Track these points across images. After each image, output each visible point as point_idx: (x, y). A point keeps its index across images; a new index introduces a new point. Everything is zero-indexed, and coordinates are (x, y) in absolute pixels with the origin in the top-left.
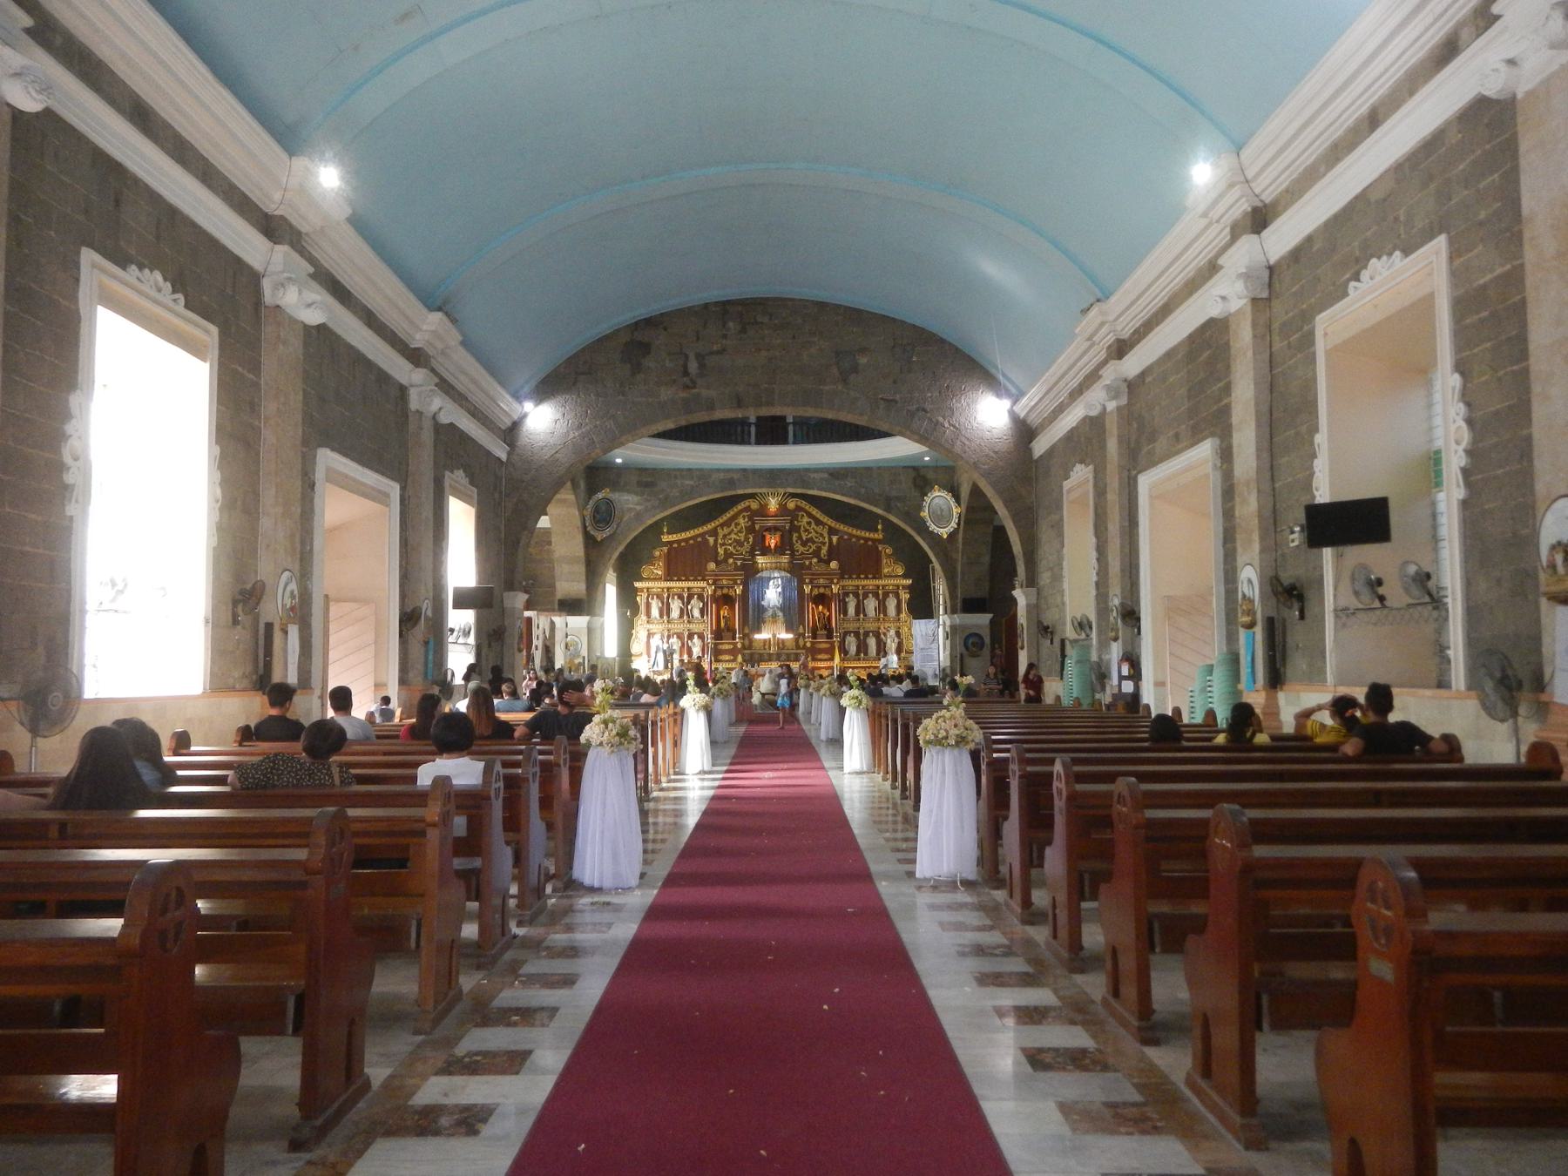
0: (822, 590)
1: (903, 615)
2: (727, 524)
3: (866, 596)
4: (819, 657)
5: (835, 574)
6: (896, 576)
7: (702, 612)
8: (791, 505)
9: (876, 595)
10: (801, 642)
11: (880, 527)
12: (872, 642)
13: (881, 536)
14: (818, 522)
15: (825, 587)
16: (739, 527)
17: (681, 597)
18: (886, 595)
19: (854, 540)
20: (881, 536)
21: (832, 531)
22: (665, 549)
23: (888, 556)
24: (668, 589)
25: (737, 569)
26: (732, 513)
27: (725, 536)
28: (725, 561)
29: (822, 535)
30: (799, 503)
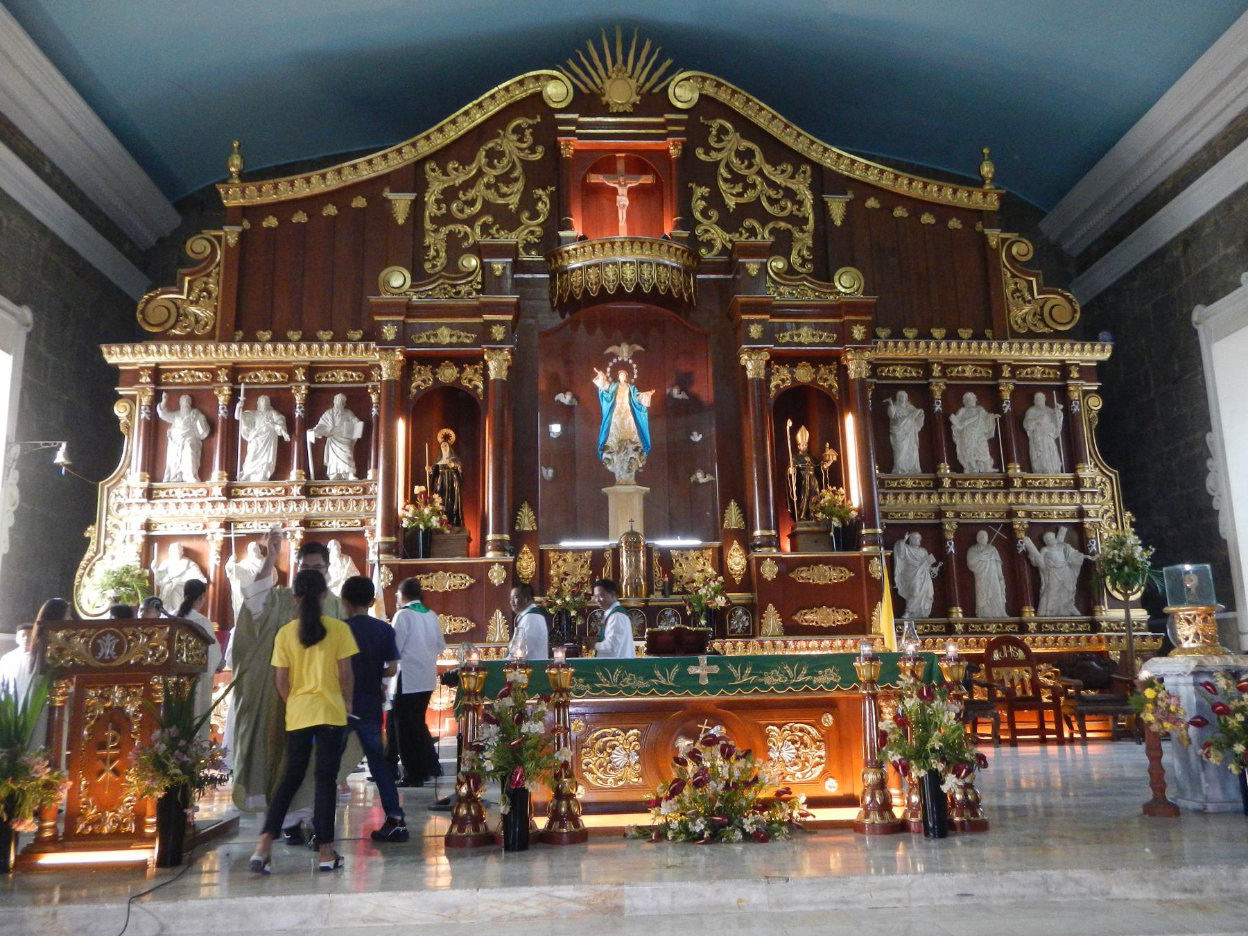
0: (804, 374)
1: (1088, 472)
2: (462, 149)
3: (954, 399)
4: (811, 617)
6: (1057, 335)
7: (361, 455)
8: (683, 93)
9: (990, 398)
11: (987, 169)
13: (993, 203)
14: (777, 152)
15: (816, 359)
16: (501, 167)
17: (281, 402)
18: (1025, 396)
19: (899, 212)
20: (993, 203)
21: (824, 181)
22: (231, 234)
23: (1025, 267)
24: (236, 371)
25: (489, 282)
27: (449, 195)
28: (452, 265)
29: (790, 194)
30: (709, 90)
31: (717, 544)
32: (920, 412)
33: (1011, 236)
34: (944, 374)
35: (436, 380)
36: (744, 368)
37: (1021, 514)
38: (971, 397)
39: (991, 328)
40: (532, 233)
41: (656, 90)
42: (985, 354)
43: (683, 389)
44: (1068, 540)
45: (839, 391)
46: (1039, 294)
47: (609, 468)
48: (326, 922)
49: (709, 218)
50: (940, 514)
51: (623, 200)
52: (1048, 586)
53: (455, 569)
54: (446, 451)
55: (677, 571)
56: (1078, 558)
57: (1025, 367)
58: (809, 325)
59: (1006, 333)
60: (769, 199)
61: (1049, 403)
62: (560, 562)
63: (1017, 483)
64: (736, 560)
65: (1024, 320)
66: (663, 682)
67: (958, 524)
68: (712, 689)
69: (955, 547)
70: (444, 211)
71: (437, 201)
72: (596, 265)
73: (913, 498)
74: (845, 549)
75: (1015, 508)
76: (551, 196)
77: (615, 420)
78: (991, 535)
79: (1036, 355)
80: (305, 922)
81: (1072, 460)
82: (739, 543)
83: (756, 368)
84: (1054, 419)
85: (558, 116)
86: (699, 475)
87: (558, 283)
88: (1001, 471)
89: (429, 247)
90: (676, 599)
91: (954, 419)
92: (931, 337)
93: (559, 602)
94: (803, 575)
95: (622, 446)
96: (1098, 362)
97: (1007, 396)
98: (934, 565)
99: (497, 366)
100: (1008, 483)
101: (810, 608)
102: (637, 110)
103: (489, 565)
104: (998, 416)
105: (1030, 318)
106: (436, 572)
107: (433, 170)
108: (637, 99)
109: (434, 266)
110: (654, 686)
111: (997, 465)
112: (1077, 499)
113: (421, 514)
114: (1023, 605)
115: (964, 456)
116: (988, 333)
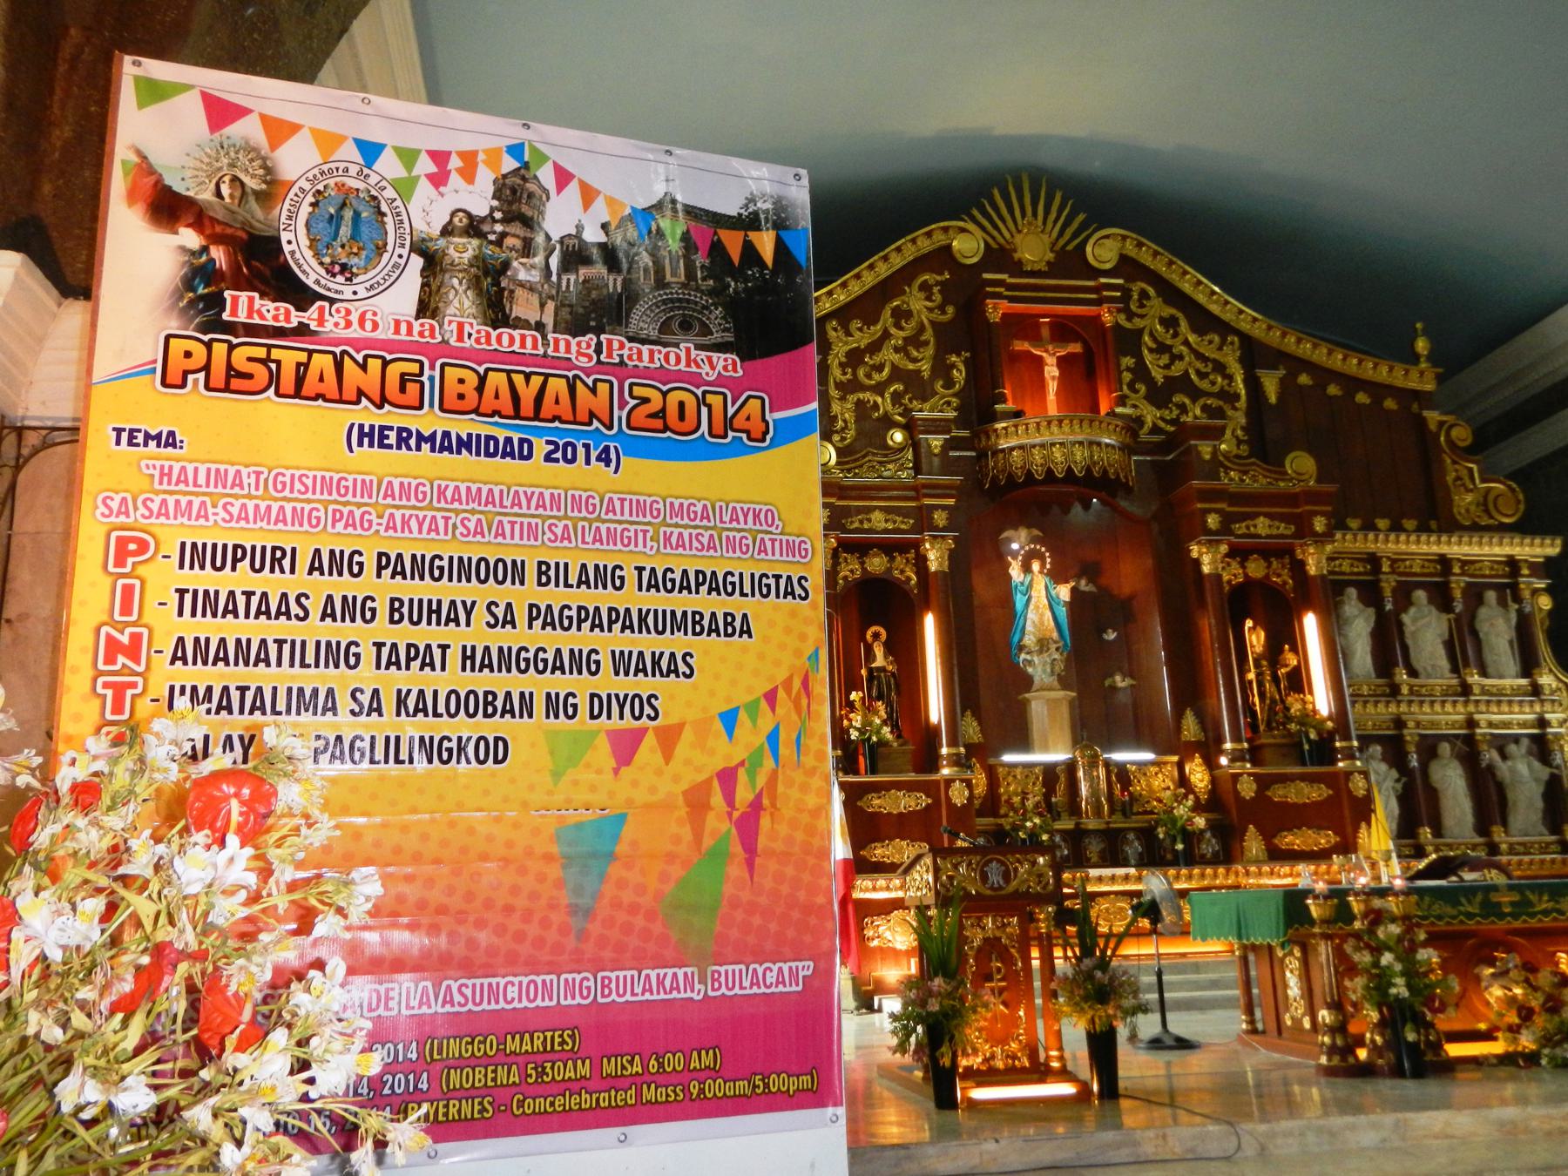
0: (1256, 569)
4: (1292, 840)
5: (1311, 497)
6: (1502, 529)
8: (1103, 251)
9: (1441, 597)
10: (1198, 775)
11: (1421, 345)
12: (1451, 780)
14: (1204, 321)
15: (1268, 552)
16: (909, 328)
18: (1475, 595)
19: (1333, 390)
21: (1255, 355)
26: (883, 270)
27: (855, 358)
29: (1220, 368)
31: (1175, 758)
32: (1371, 611)
33: (1449, 418)
34: (1393, 572)
35: (864, 570)
36: (1197, 563)
37: (1483, 724)
38: (1420, 595)
39: (1437, 519)
40: (949, 403)
41: (1070, 248)
42: (1435, 549)
43: (1090, 581)
44: (1530, 753)
45: (1295, 590)
46: (1483, 481)
47: (1030, 670)
48: (1404, 1139)
49: (1136, 391)
50: (1399, 723)
51: (1051, 371)
52: (1515, 803)
53: (910, 787)
54: (879, 651)
55: (1136, 789)
56: (1544, 773)
57: (1473, 562)
58: (1266, 515)
59: (1450, 526)
60: (1198, 372)
61: (1502, 603)
62: (1010, 779)
63: (1476, 690)
64: (1198, 775)
65: (1468, 511)
66: (1470, 909)
67: (1421, 736)
68: (1515, 916)
69: (1419, 760)
70: (849, 376)
71: (841, 365)
72: (1043, 446)
73: (1370, 708)
74: (1321, 764)
75: (1477, 717)
76: (966, 362)
77: (1031, 615)
78: (1453, 746)
79: (1486, 550)
80: (1384, 1140)
81: (1528, 665)
82: (1202, 757)
83: (1213, 562)
84: (1508, 620)
85: (986, 276)
86: (1118, 678)
87: (991, 464)
88: (1460, 677)
89: (836, 417)
90: (1136, 822)
91: (1406, 618)
92: (1374, 528)
93: (1028, 824)
94: (1280, 792)
95: (1043, 644)
96: (1549, 559)
97: (1458, 594)
98: (1397, 781)
99: (935, 558)
100: (1466, 690)
101: (1290, 830)
102: (1054, 269)
103: (949, 782)
104: (1452, 616)
105: (1473, 508)
106: (888, 790)
107: (835, 329)
108: (1050, 256)
109: (843, 439)
110: (1461, 913)
111: (1455, 670)
112: (1537, 708)
113: (870, 724)
114: (1493, 823)
115: (1419, 662)
116: (1433, 525)
